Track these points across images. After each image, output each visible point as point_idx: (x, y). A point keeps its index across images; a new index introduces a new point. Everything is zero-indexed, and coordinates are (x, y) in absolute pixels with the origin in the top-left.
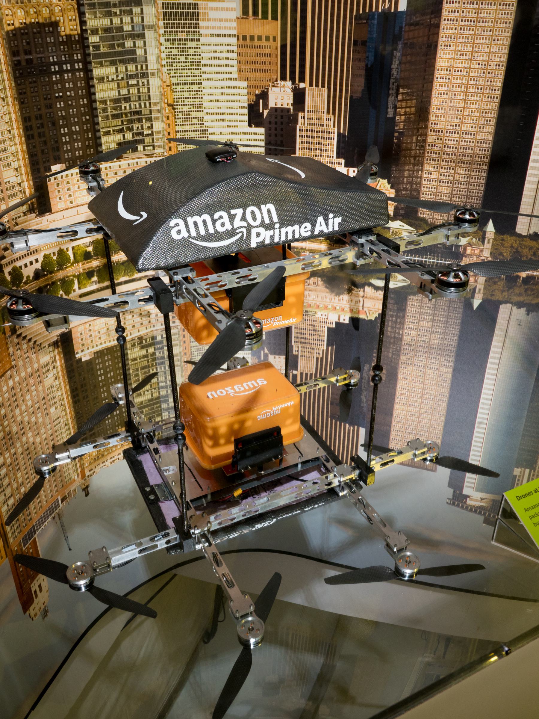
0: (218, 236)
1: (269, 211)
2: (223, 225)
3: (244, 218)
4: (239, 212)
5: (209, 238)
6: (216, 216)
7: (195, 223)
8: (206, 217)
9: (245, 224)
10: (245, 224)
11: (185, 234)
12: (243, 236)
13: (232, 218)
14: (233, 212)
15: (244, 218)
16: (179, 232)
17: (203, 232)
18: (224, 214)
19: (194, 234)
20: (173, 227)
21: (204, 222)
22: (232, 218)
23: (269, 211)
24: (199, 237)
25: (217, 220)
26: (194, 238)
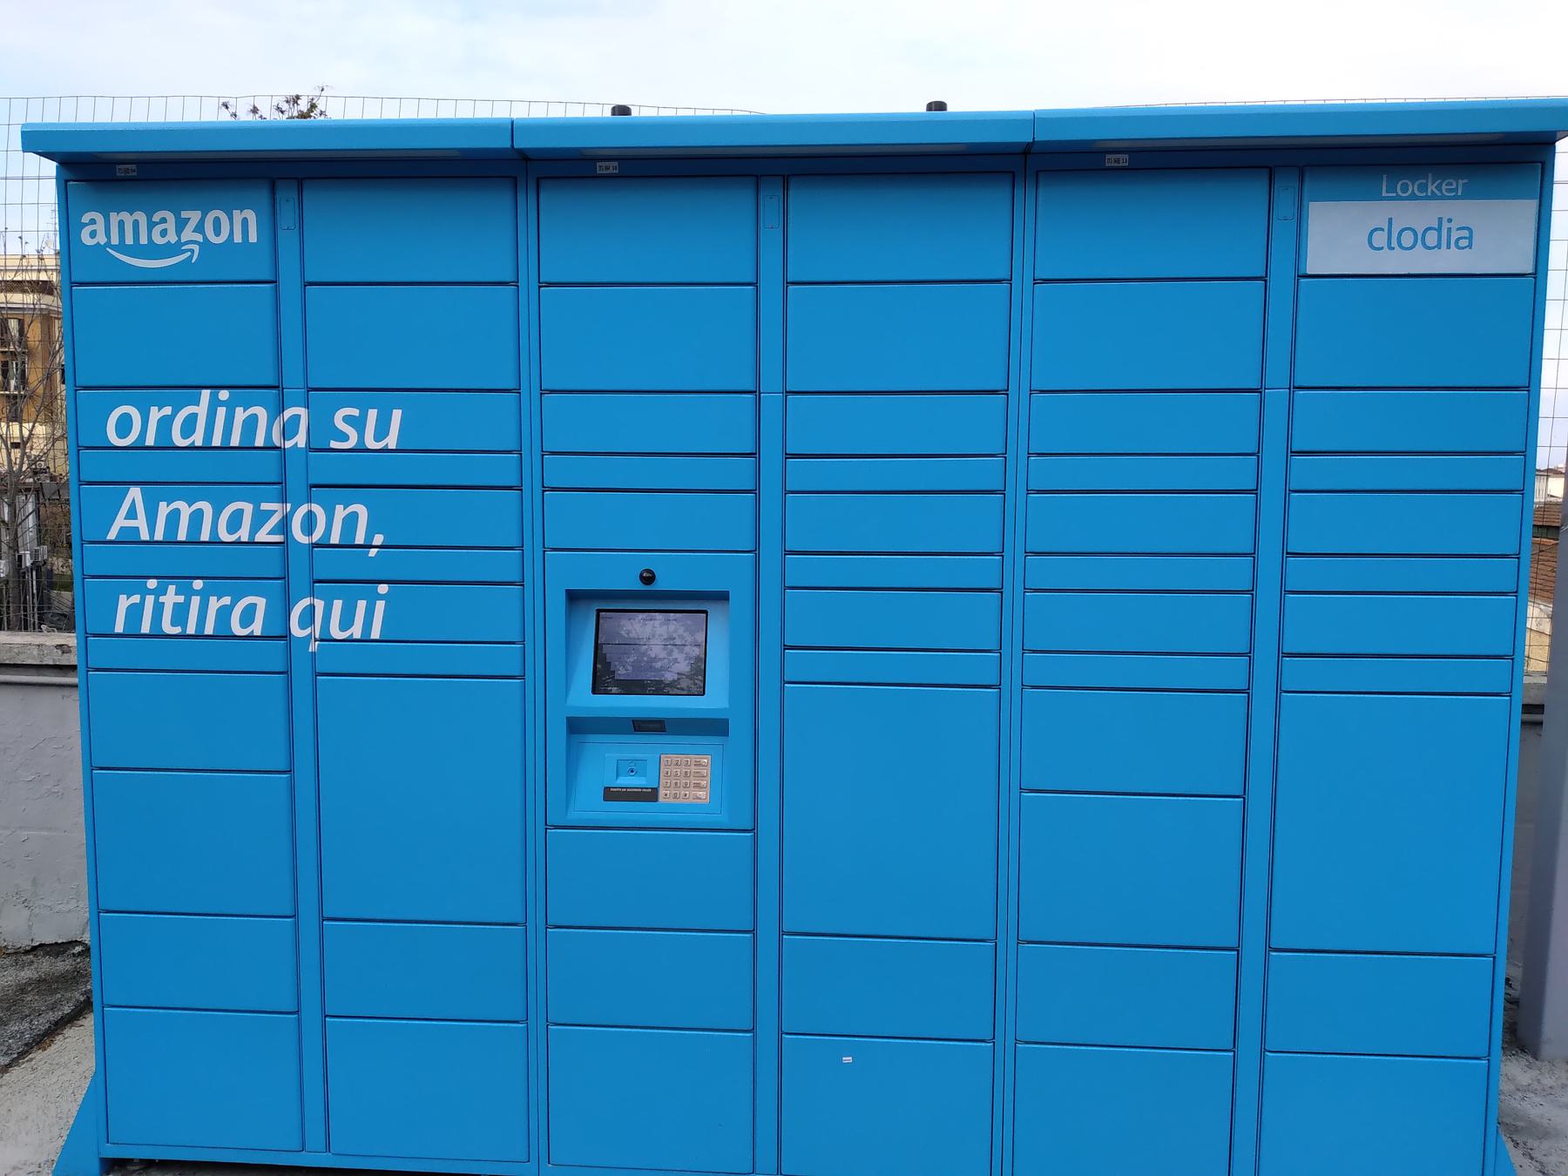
0: (153, 251)
1: (245, 221)
2: (164, 233)
3: (200, 228)
4: (194, 216)
5: (137, 250)
6: (156, 218)
7: (121, 224)
8: (141, 217)
9: (199, 238)
10: (199, 238)
11: (101, 239)
12: (191, 257)
13: (181, 224)
14: (184, 214)
15: (200, 228)
16: (93, 234)
17: (129, 240)
18: (169, 216)
19: (115, 241)
20: (87, 225)
21: (136, 224)
22: (181, 224)
23: (245, 221)
24: (121, 247)
25: (158, 223)
26: (114, 248)
